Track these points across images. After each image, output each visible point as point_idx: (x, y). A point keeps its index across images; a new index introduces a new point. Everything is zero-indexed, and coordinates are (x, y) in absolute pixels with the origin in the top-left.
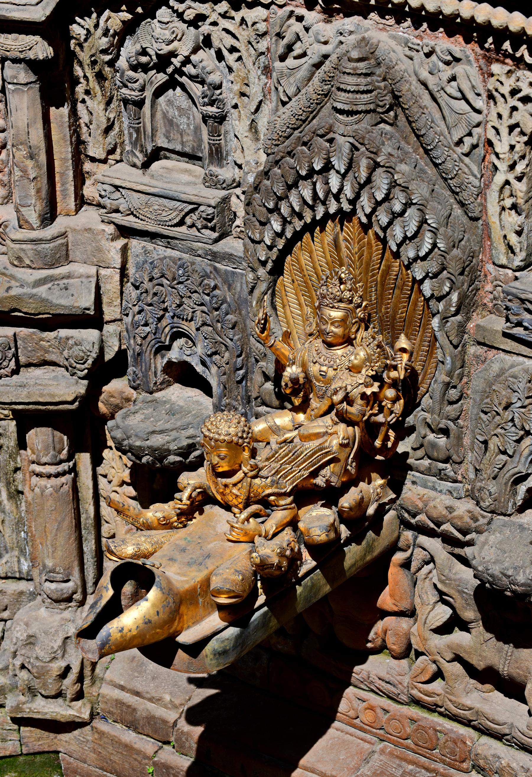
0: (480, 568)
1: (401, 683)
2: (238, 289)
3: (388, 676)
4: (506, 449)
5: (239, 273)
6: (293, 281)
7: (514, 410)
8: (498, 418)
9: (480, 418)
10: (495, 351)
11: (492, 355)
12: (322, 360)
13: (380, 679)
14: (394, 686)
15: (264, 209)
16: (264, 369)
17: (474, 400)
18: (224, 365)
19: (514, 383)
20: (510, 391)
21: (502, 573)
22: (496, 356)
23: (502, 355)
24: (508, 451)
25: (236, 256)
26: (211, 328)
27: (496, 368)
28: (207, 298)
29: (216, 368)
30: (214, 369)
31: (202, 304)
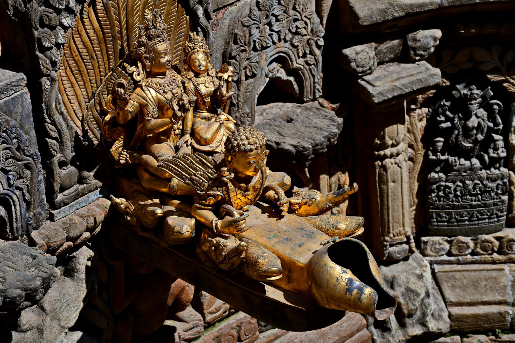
0: (311, 147)
1: (200, 320)
2: (20, 110)
3: (191, 323)
4: (253, 73)
5: (19, 95)
6: (66, 68)
7: (255, 39)
8: (243, 55)
9: (234, 63)
10: (222, 11)
11: (222, 14)
12: (167, 87)
13: (186, 331)
14: (197, 326)
15: (55, 14)
16: (63, 159)
17: (216, 58)
18: (28, 183)
19: (248, 21)
20: (245, 28)
21: (324, 137)
22: (226, 13)
23: (230, 8)
24: (256, 72)
25: (14, 82)
26: (11, 160)
27: (227, 22)
28: (4, 134)
29: (18, 192)
30: (16, 196)
31: (3, 143)
